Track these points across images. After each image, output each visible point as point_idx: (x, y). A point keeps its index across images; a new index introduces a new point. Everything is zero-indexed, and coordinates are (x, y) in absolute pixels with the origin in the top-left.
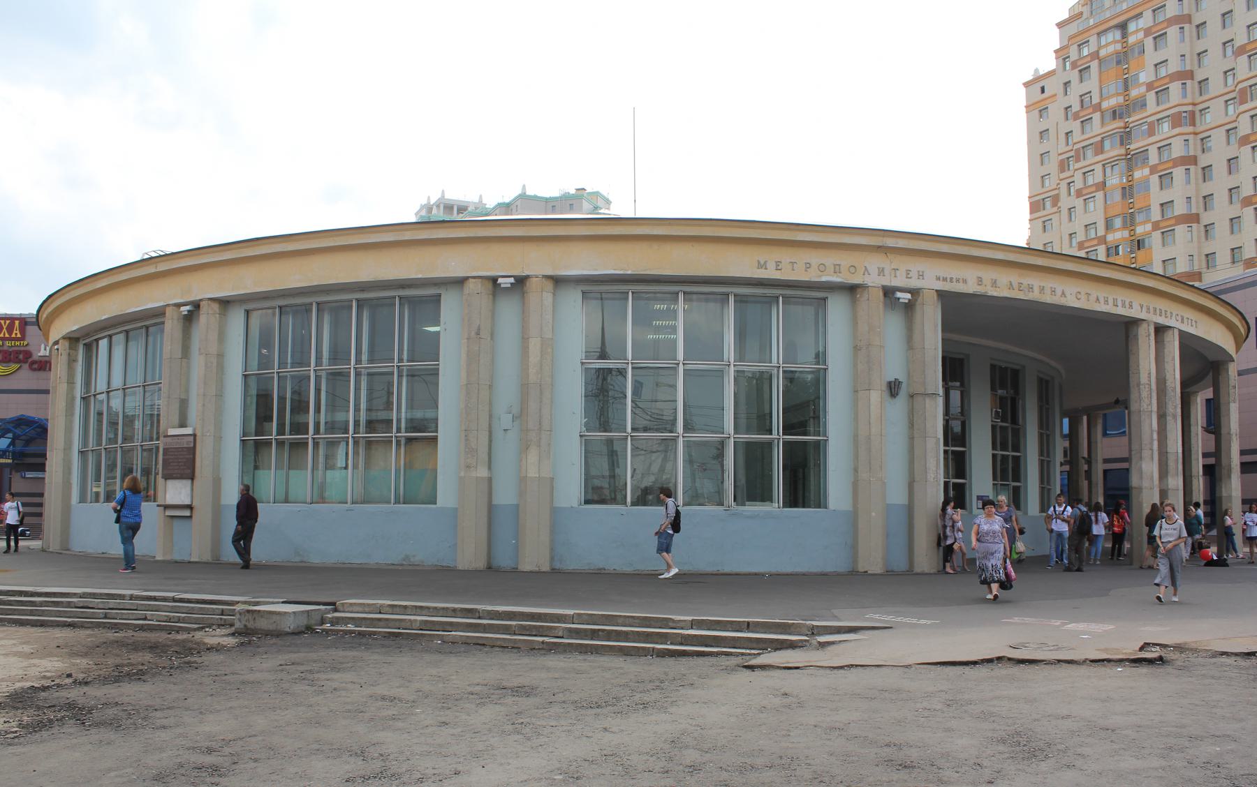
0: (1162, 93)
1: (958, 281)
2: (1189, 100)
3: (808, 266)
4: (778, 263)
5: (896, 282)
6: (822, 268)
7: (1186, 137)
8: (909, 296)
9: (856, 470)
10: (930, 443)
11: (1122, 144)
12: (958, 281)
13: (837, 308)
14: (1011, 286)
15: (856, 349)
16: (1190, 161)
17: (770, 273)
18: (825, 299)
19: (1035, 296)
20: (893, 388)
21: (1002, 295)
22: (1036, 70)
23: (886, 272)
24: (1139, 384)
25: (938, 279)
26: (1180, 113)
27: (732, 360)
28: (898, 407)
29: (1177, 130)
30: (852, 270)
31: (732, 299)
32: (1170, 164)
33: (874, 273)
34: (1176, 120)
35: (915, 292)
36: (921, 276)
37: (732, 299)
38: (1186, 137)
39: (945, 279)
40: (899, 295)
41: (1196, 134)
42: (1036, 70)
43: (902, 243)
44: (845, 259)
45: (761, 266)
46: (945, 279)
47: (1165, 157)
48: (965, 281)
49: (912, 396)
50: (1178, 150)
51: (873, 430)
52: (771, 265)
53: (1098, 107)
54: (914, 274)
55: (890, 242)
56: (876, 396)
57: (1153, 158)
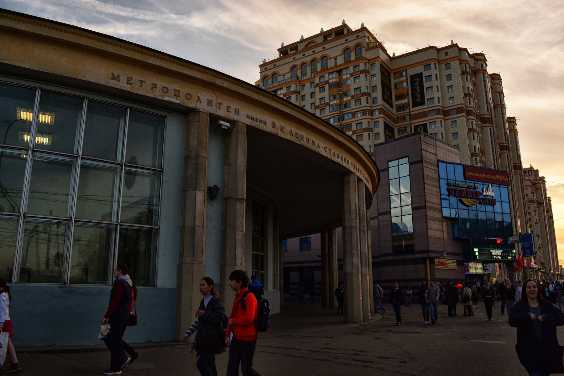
0: (358, 100)
1: (261, 121)
2: (369, 105)
3: (154, 86)
4: (129, 79)
5: (222, 112)
6: (165, 90)
7: (369, 120)
8: (228, 125)
9: (181, 255)
10: (239, 236)
11: (339, 121)
12: (261, 121)
13: (173, 130)
14: (291, 133)
15: (187, 158)
16: (369, 130)
17: (122, 85)
18: (165, 117)
19: (304, 143)
20: (212, 193)
21: (286, 138)
22: (302, 36)
23: (214, 104)
24: (350, 210)
25: (248, 117)
26: (366, 109)
27: (80, 153)
28: (214, 209)
29: (365, 117)
30: (188, 97)
31: (85, 104)
32: (362, 131)
33: (204, 101)
34: (364, 112)
35: (233, 123)
36: (237, 112)
37: (85, 104)
38: (369, 120)
39: (252, 119)
40: (222, 122)
41: (372, 119)
42: (302, 36)
43: (226, 85)
44: (184, 89)
45: (113, 77)
46: (252, 119)
47: (359, 128)
48: (265, 123)
49: (226, 199)
50: (365, 125)
51: (197, 222)
52: (123, 79)
53: (328, 104)
54: (232, 110)
55: (219, 82)
56: (200, 196)
57: (354, 127)
